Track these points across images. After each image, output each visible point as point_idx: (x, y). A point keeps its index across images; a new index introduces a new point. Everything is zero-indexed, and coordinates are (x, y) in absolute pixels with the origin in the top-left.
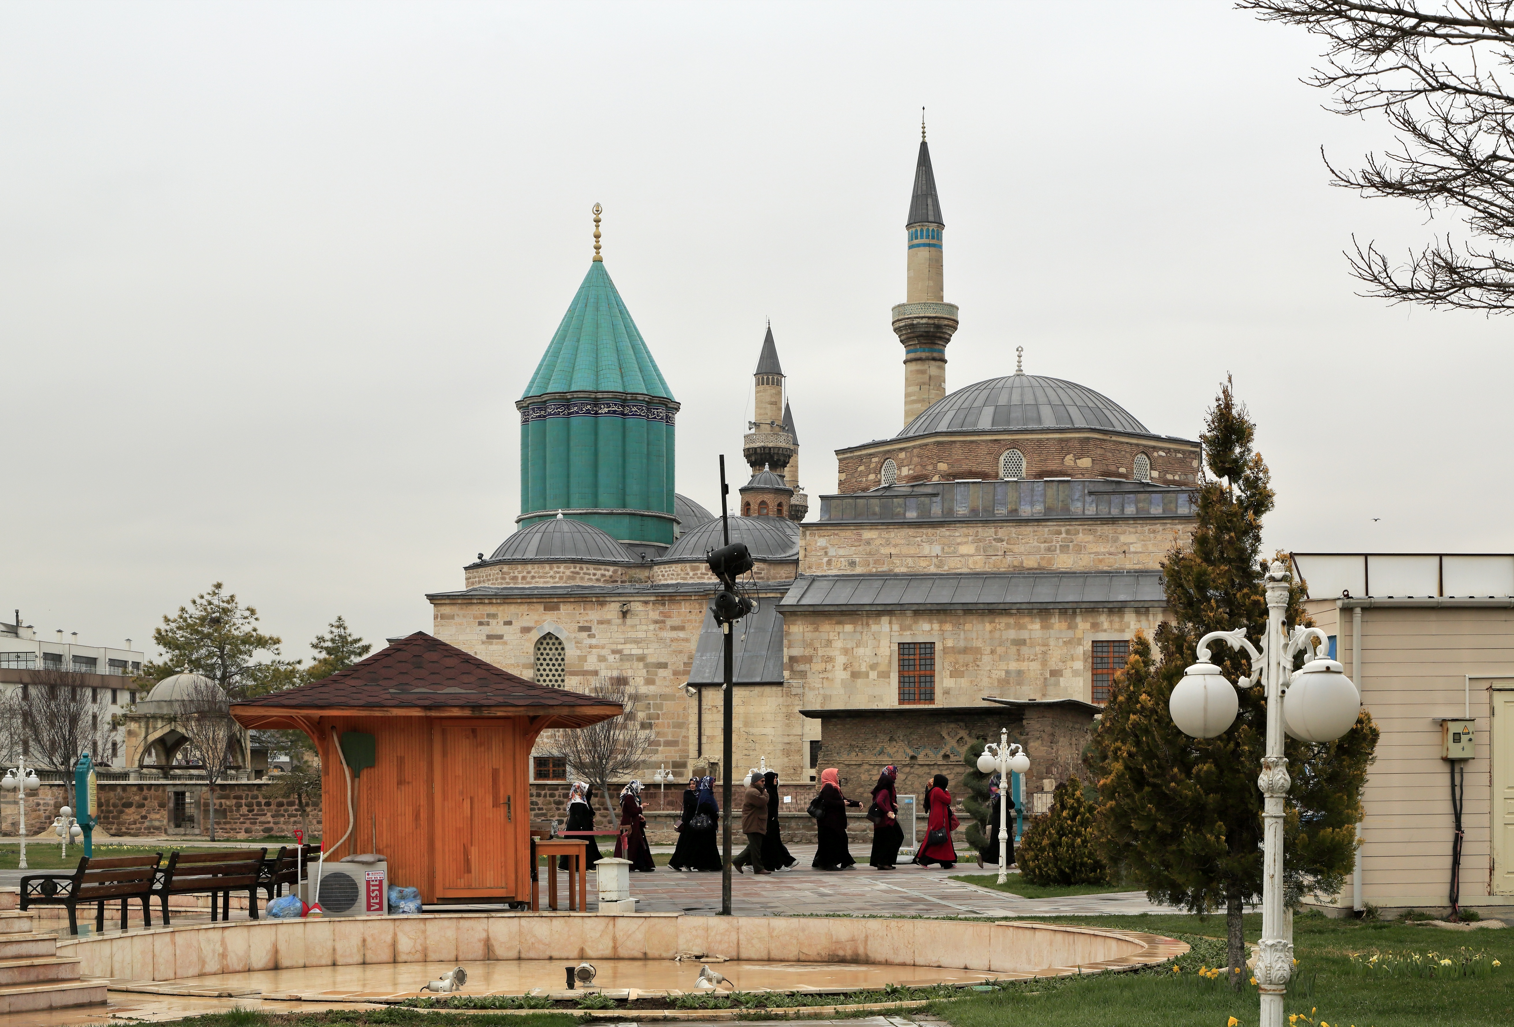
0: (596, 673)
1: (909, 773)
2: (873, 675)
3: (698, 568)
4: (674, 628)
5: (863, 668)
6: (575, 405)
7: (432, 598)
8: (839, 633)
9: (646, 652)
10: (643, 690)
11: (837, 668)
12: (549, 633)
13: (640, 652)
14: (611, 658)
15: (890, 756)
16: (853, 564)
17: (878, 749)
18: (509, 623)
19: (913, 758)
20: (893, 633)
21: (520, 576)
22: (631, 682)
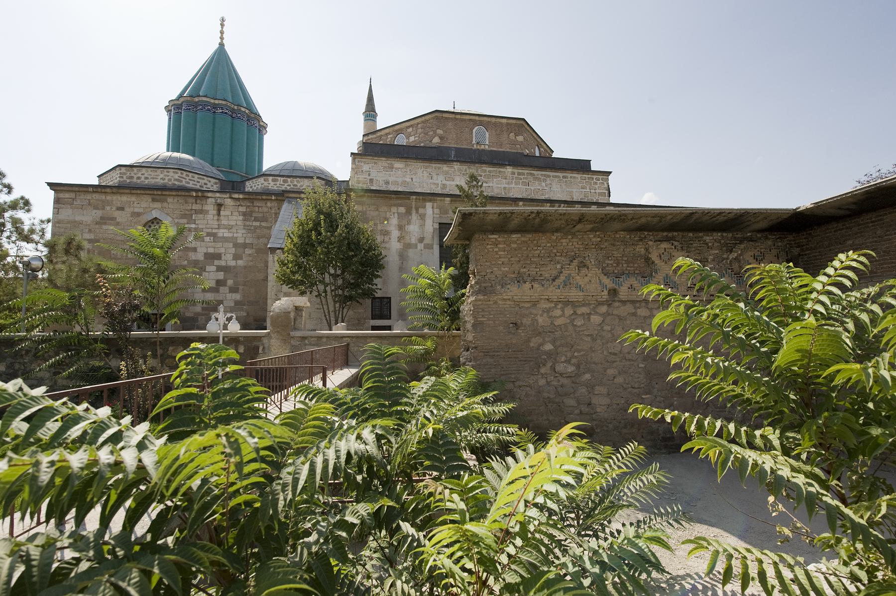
0: (195, 250)
1: (605, 315)
2: (420, 246)
3: (277, 180)
4: (256, 219)
5: (413, 241)
6: (201, 105)
7: (52, 185)
8: (394, 213)
9: (235, 235)
10: (232, 263)
11: (392, 240)
12: (156, 218)
13: (230, 235)
14: (207, 239)
15: (580, 288)
16: (387, 183)
17: (562, 278)
18: (122, 209)
19: (613, 292)
20: (435, 216)
21: (135, 177)
22: (223, 257)
